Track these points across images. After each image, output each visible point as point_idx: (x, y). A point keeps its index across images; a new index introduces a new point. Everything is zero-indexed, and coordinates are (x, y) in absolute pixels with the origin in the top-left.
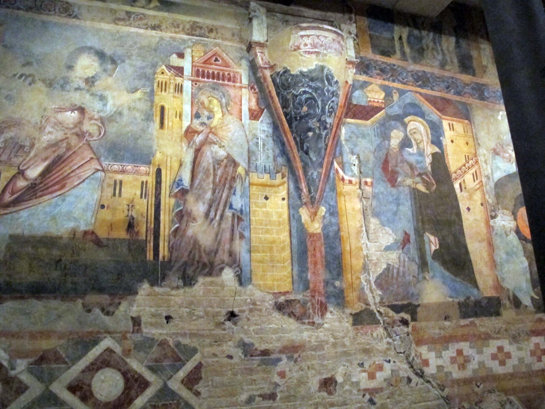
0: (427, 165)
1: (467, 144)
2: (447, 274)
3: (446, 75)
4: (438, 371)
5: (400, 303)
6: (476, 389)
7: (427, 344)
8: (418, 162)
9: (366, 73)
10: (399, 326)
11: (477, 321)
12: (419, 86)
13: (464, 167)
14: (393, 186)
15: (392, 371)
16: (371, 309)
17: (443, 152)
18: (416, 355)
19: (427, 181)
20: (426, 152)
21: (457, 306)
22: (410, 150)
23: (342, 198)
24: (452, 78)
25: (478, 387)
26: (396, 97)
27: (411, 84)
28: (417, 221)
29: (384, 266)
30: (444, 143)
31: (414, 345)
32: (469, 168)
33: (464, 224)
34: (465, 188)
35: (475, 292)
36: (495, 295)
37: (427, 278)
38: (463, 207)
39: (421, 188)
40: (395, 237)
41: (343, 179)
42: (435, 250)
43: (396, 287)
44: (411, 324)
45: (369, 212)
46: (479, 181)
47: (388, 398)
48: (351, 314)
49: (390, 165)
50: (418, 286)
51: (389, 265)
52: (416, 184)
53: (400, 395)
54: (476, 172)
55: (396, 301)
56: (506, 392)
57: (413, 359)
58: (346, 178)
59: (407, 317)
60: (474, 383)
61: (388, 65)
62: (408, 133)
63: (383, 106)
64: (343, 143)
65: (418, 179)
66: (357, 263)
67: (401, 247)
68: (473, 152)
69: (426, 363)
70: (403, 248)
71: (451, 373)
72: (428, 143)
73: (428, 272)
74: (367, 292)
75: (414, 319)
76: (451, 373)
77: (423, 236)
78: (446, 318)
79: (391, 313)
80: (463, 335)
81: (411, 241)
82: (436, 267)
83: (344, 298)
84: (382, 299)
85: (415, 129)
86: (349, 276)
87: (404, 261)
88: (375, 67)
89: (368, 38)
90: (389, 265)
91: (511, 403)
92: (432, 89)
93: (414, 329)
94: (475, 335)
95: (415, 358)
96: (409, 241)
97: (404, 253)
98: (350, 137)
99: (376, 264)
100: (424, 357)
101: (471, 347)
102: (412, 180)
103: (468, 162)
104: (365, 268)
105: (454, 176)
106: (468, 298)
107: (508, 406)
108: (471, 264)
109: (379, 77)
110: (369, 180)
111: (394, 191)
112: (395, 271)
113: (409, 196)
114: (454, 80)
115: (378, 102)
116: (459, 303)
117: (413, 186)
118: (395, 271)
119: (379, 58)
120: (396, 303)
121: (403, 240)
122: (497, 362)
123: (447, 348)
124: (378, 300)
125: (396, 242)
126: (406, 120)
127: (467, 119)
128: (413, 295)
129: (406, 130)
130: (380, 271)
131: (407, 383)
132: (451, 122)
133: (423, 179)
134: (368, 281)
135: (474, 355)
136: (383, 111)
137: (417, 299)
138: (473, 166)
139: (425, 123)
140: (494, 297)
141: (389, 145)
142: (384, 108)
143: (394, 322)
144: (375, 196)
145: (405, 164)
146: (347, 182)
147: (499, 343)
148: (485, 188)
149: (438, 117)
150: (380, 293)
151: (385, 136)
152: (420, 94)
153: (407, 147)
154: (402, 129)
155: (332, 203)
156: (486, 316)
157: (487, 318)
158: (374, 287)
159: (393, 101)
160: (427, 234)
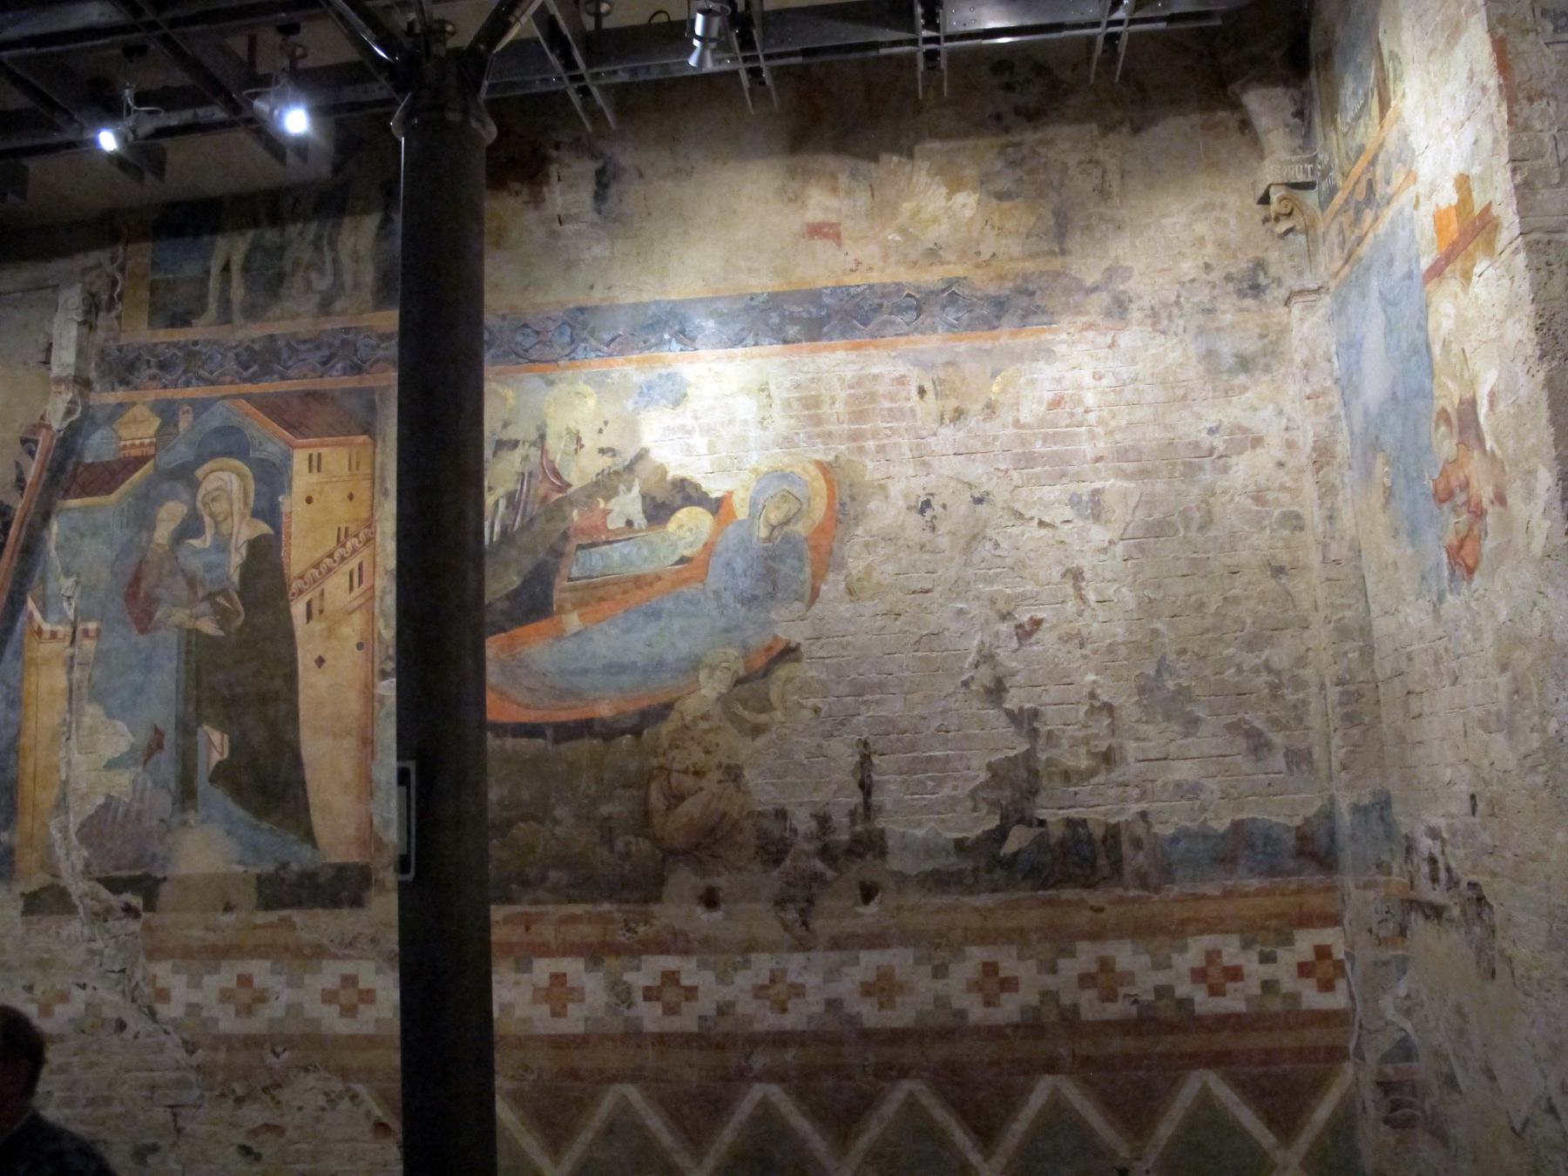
0: (232, 570)
1: (351, 497)
2: (239, 812)
3: (328, 327)
4: (187, 1014)
5: (125, 874)
6: (271, 1059)
7: (172, 957)
8: (209, 567)
9: (125, 382)
10: (119, 919)
11: (297, 916)
12: (252, 379)
13: (327, 560)
14: (142, 631)
15: (88, 1005)
16: (62, 884)
17: (278, 532)
18: (144, 979)
19: (225, 610)
20: (233, 541)
21: (254, 882)
22: (195, 542)
23: (33, 670)
24: (347, 330)
25: (277, 1055)
26: (184, 423)
27: (228, 379)
28: (186, 701)
29: (101, 800)
30: (285, 509)
31: (142, 959)
32: (343, 559)
33: (302, 697)
34: (321, 612)
35: (305, 851)
36: (357, 859)
37: (192, 822)
38: (305, 659)
39: (208, 627)
40: (132, 739)
41: (40, 632)
42: (220, 763)
43: (118, 842)
44: (145, 915)
45: (85, 691)
46: (364, 587)
47: (75, 1054)
48: (23, 894)
49: (144, 585)
50: (169, 839)
51: (109, 797)
52: (197, 618)
53: (99, 1052)
54: (360, 567)
55: (118, 868)
56: (345, 1074)
57: (137, 984)
58: (47, 627)
59: (136, 901)
60: (268, 1046)
61: (180, 349)
62: (199, 505)
63: (152, 451)
64: (53, 553)
65: (205, 607)
66: (48, 797)
67: (142, 759)
68: (365, 515)
69: (163, 995)
70: (145, 762)
71: (216, 1021)
72: (243, 516)
73: (196, 811)
74: (60, 852)
75: (150, 906)
76: (216, 1021)
77: (195, 733)
78: (228, 908)
79: (105, 893)
80: (256, 947)
81: (166, 747)
82: (216, 798)
83: (12, 864)
84: (87, 865)
85: (217, 489)
86: (28, 819)
87: (144, 789)
88: (148, 362)
89: (144, 294)
90: (109, 797)
91: (354, 1097)
92: (283, 378)
93: (147, 928)
94: (286, 948)
95: (142, 984)
96: (160, 746)
97: (145, 770)
98: (67, 539)
99: (83, 798)
100: (161, 984)
101: (273, 972)
102: (188, 612)
103: (344, 546)
104: (62, 805)
105: (295, 586)
106: (285, 865)
107: (345, 1104)
108: (305, 791)
109: (155, 383)
110: (92, 626)
111: (143, 641)
112: (121, 810)
113: (174, 652)
114: (350, 337)
115: (142, 445)
116: (259, 877)
117: (189, 625)
118: (121, 810)
119: (164, 336)
120: (118, 874)
121: (150, 746)
122: (334, 1010)
123: (217, 970)
124: (80, 866)
125: (133, 748)
126: (199, 473)
127: (365, 432)
128: (154, 857)
129: (194, 496)
130: (89, 809)
131: (116, 1032)
132: (314, 451)
133: (215, 604)
134: (64, 830)
135: (278, 988)
136: (150, 464)
137: (163, 866)
138: (355, 551)
139: (246, 469)
140: (355, 865)
141: (150, 540)
142: (153, 456)
143: (109, 910)
144: (101, 658)
145: (180, 577)
146: (48, 636)
147: (348, 968)
148: (377, 605)
149: (282, 445)
150: (86, 854)
151: (143, 518)
152: (248, 398)
153: (191, 537)
154: (186, 497)
155: (12, 683)
156: (324, 906)
157: (327, 911)
158: (74, 840)
159: (178, 433)
160: (206, 727)
